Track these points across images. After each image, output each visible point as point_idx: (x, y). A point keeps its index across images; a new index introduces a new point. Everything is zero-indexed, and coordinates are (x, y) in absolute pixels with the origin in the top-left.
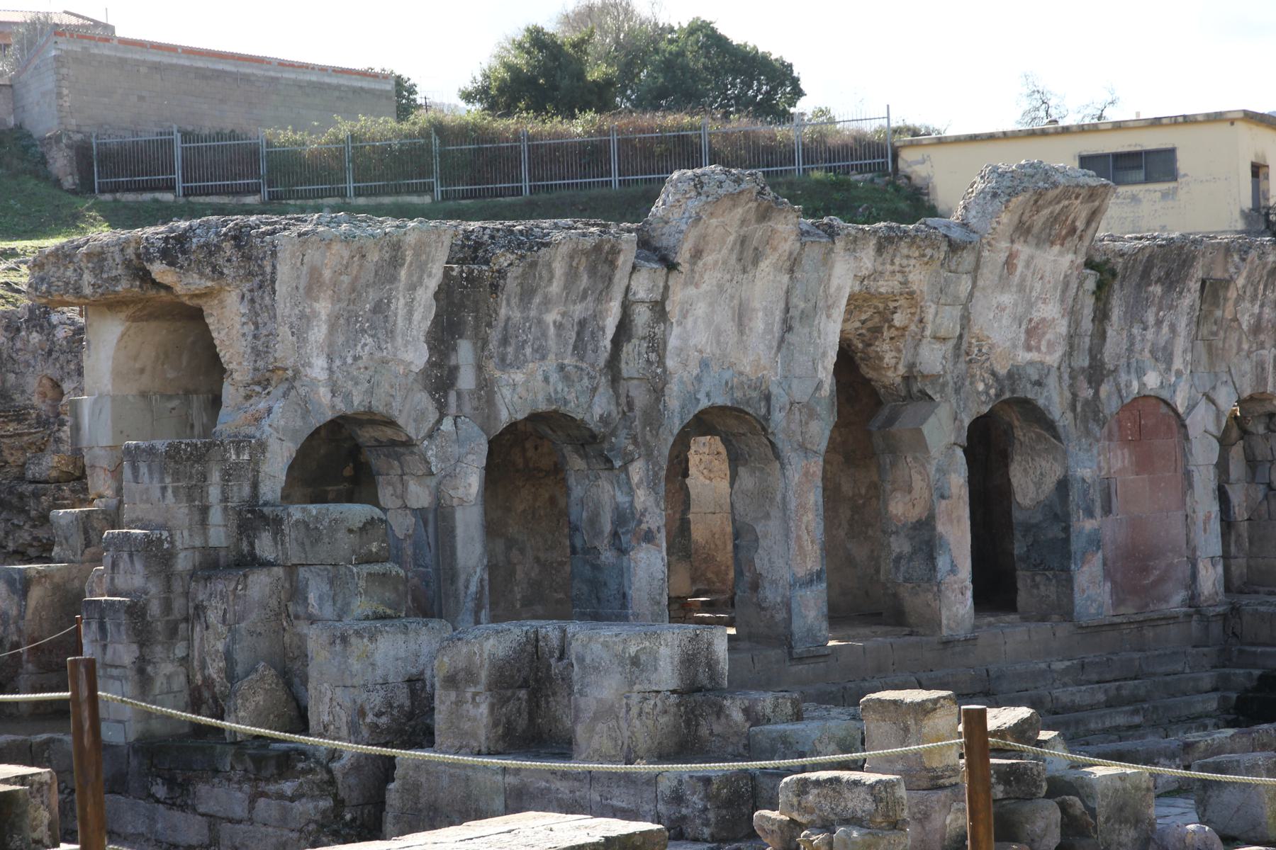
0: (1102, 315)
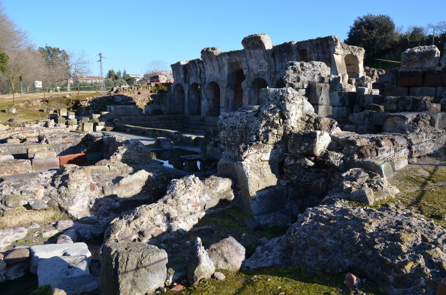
0: (275, 61)
